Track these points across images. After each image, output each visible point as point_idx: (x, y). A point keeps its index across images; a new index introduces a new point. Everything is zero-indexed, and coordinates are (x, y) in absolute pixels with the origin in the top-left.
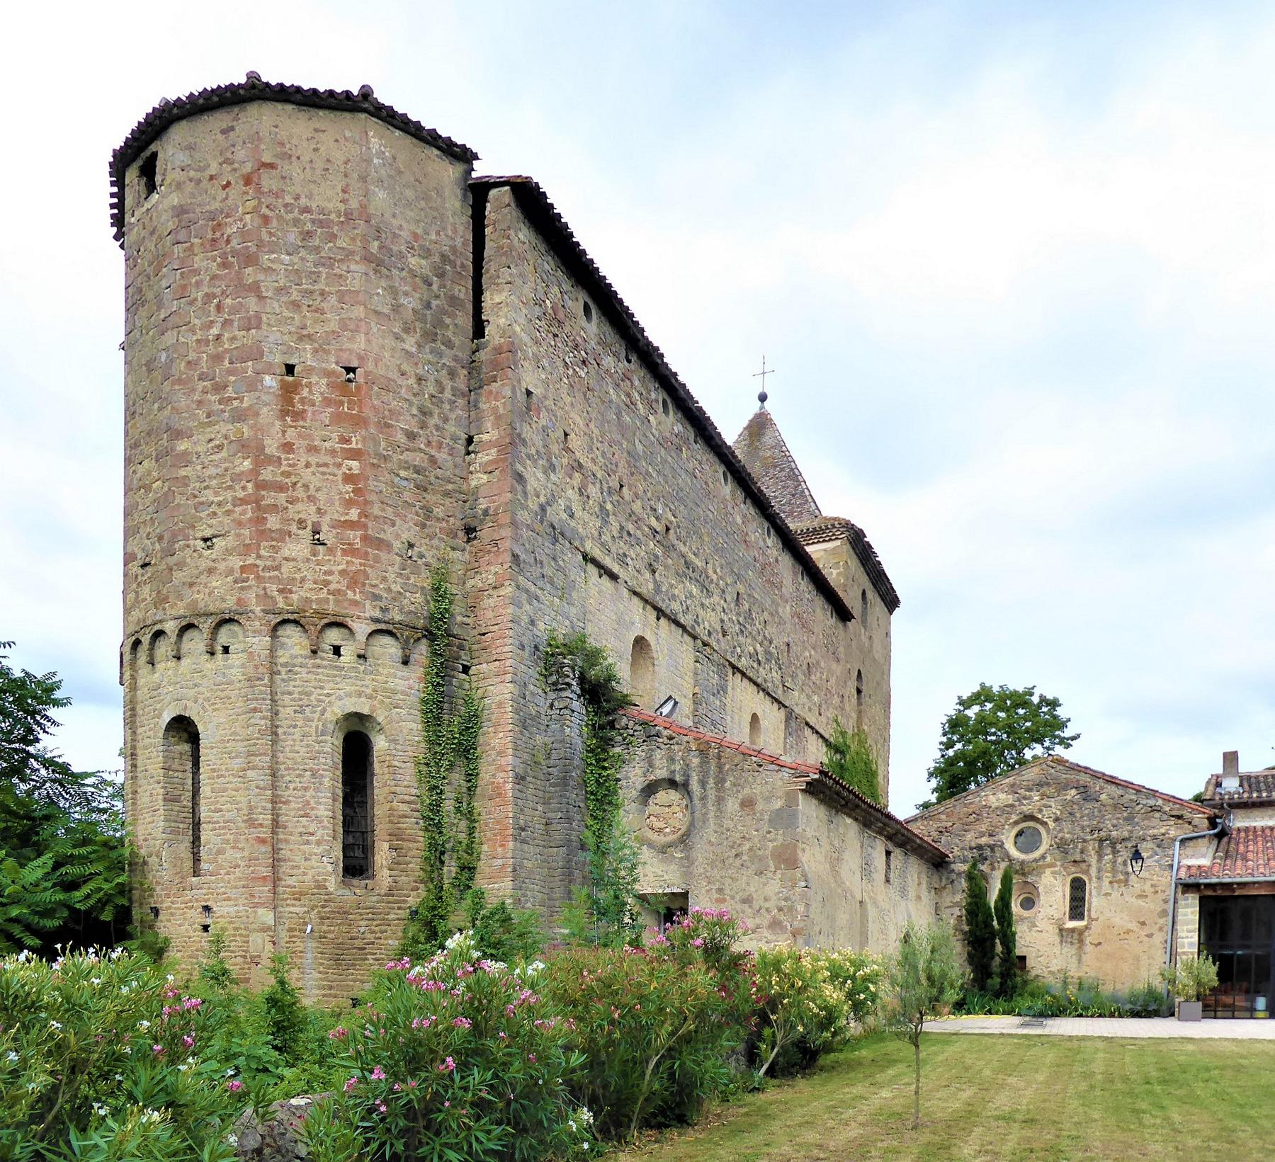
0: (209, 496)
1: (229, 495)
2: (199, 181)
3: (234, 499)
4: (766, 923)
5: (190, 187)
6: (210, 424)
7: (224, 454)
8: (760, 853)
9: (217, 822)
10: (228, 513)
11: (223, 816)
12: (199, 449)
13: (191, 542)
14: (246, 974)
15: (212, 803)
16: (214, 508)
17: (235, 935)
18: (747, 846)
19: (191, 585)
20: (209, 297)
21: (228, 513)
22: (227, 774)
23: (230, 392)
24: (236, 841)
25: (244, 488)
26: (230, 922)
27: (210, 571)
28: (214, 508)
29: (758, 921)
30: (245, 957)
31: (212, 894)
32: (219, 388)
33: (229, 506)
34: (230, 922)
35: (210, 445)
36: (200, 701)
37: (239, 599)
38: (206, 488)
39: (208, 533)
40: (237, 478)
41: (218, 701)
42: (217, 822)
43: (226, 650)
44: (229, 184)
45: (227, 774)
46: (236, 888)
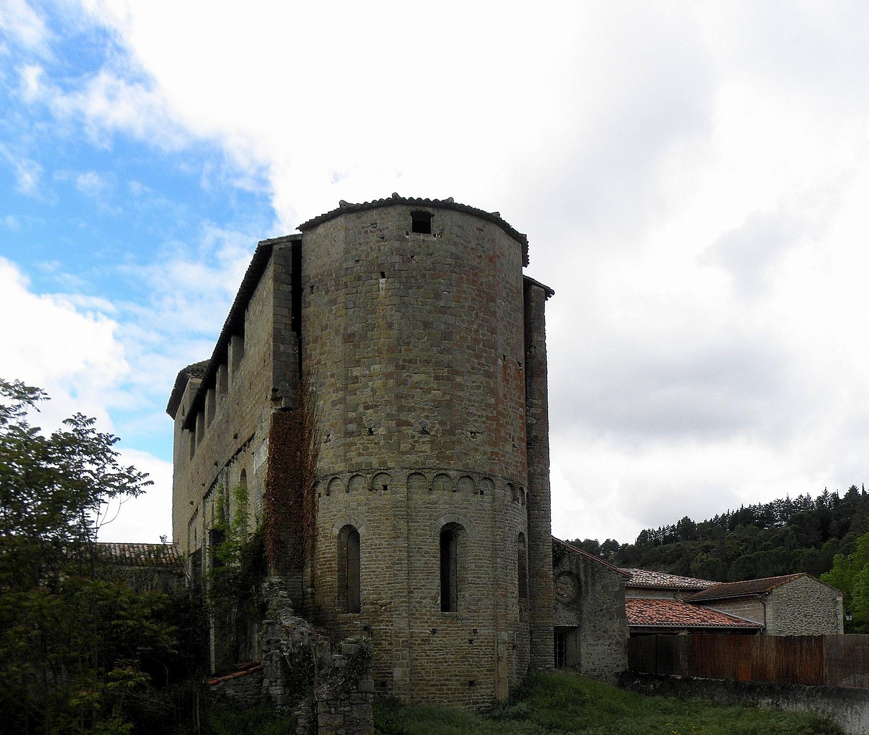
0: (472, 410)
1: (484, 413)
2: (465, 247)
3: (487, 416)
4: (614, 642)
5: (461, 247)
6: (474, 374)
7: (481, 391)
8: (611, 610)
9: (479, 584)
10: (484, 422)
11: (482, 581)
12: (468, 384)
13: (465, 432)
14: (493, 666)
15: (475, 573)
16: (476, 417)
17: (488, 646)
18: (605, 606)
19: (466, 454)
20: (471, 308)
21: (484, 422)
22: (483, 558)
23: (483, 361)
24: (488, 595)
25: (492, 412)
26: (486, 639)
27: (476, 450)
28: (476, 417)
29: (611, 641)
30: (492, 658)
31: (476, 623)
32: (479, 357)
33: (484, 419)
34: (486, 639)
35: (474, 384)
36: (468, 517)
37: (491, 468)
38: (472, 406)
39: (474, 430)
40: (488, 405)
41: (478, 519)
42: (479, 584)
43: (482, 493)
44: (480, 257)
45: (483, 558)
46: (488, 620)
